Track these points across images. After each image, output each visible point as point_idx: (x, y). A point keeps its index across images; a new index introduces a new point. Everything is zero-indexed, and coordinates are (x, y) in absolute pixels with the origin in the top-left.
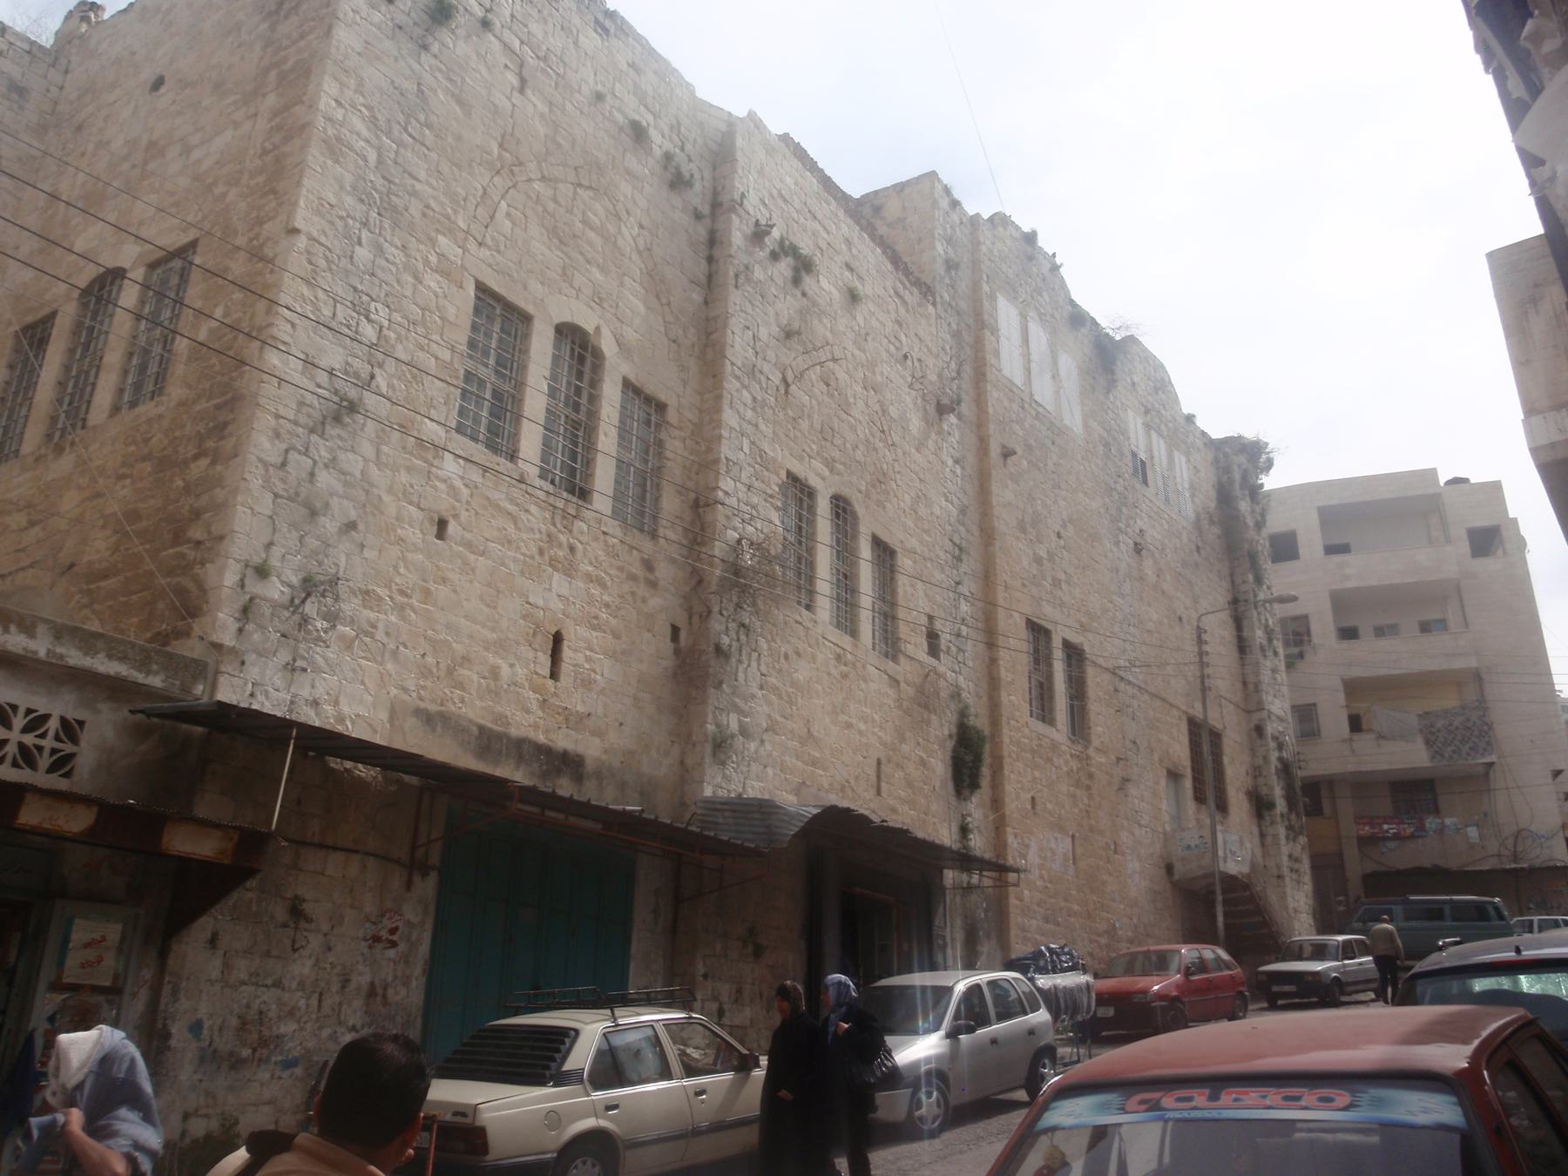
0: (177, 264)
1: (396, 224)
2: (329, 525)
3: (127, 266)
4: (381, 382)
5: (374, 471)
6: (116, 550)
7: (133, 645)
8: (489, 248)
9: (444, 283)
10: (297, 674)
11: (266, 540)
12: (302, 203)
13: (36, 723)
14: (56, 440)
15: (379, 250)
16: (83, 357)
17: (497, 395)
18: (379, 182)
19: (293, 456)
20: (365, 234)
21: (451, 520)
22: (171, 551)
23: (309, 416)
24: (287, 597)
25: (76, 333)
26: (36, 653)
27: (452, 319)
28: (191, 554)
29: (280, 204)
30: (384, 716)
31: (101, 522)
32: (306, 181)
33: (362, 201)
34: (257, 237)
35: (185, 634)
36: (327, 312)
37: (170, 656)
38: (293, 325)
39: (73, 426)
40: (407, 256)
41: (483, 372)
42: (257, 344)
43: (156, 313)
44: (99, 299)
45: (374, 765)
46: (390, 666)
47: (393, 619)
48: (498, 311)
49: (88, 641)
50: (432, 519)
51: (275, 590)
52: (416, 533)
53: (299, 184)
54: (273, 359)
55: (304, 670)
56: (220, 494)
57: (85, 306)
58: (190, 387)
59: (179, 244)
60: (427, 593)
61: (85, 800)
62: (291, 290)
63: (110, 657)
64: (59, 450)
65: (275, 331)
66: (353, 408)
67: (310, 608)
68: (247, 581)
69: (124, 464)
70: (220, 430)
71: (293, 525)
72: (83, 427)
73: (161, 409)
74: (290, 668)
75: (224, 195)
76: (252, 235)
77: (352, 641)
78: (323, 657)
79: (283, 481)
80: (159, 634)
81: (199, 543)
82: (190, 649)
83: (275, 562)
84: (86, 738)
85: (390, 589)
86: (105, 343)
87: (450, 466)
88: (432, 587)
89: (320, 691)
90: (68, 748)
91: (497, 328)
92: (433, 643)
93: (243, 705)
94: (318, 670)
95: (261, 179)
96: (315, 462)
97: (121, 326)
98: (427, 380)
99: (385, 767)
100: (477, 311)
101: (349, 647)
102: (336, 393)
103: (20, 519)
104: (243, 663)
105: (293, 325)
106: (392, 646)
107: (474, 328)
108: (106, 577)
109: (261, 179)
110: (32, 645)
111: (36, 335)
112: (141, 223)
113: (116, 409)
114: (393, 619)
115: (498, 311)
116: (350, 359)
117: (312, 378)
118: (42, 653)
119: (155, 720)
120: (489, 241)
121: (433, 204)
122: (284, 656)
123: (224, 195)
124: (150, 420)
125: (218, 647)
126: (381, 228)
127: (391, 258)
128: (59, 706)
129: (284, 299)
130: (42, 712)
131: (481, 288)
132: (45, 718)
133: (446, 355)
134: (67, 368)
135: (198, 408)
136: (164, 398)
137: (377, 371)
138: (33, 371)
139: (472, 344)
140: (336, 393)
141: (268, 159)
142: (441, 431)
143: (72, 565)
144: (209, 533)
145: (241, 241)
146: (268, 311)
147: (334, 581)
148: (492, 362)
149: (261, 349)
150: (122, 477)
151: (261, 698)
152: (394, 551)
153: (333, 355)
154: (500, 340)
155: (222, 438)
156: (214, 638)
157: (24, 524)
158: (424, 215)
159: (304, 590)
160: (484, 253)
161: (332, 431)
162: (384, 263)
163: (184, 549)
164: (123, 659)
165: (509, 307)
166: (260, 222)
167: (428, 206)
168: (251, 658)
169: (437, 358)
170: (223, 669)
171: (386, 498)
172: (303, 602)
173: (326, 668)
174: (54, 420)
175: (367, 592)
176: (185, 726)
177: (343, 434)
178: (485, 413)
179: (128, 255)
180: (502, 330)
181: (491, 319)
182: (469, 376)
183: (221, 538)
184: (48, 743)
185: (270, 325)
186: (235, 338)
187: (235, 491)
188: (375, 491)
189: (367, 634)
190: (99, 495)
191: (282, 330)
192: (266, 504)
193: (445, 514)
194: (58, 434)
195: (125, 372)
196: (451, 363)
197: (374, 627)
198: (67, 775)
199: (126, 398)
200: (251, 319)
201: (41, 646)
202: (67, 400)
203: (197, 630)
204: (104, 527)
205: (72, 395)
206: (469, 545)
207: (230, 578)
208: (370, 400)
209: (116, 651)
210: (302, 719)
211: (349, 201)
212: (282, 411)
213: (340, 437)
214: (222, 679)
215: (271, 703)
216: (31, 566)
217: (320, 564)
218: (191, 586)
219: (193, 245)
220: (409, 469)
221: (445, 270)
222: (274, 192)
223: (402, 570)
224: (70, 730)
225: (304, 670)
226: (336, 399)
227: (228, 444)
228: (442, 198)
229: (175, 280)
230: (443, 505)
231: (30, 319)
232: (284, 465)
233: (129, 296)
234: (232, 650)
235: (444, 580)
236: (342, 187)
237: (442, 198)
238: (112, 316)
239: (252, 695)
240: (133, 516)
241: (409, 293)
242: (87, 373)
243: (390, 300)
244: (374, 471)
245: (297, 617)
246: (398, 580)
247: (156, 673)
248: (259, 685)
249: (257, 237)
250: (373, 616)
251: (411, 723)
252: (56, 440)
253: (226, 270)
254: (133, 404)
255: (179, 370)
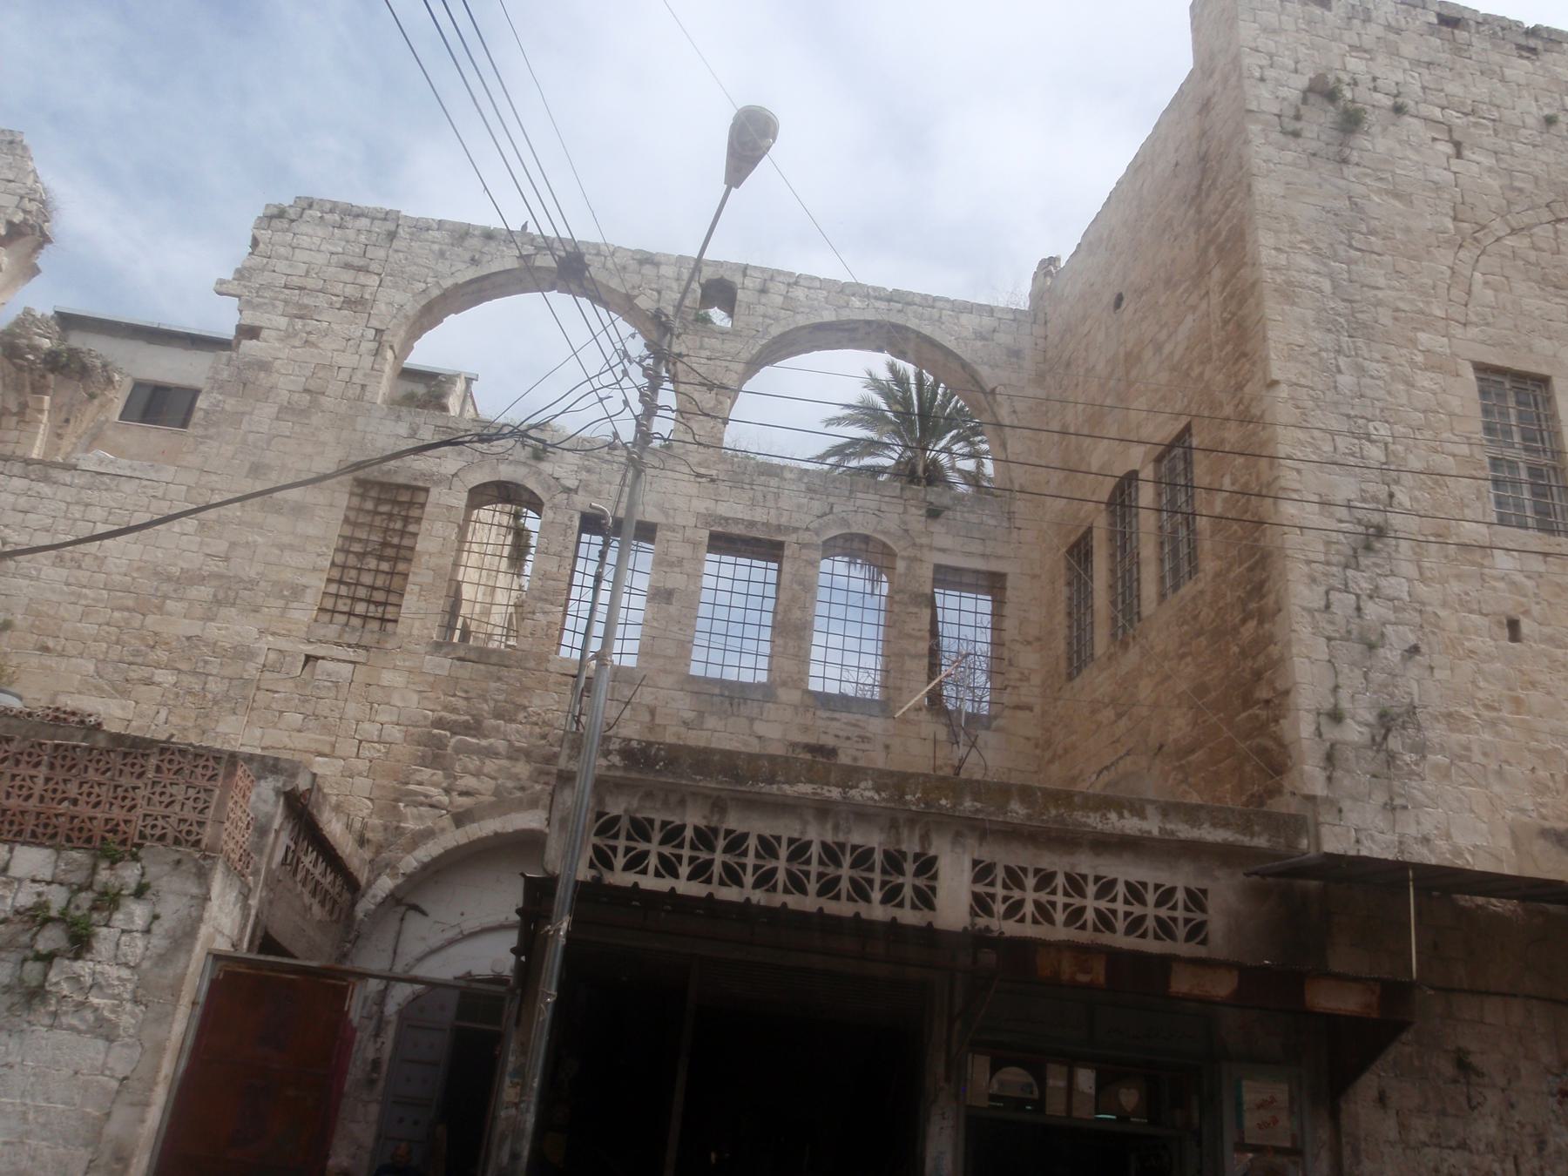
0: (1178, 451)
1: (1370, 339)
2: (1391, 655)
3: (1137, 467)
4: (1402, 497)
5: (1422, 590)
6: (1195, 724)
7: (1233, 811)
8: (1477, 325)
9: (1439, 377)
10: (1398, 813)
11: (1331, 685)
12: (1272, 355)
13: (1166, 896)
14: (1122, 637)
15: (1361, 370)
16: (1123, 558)
17: (1535, 472)
18: (1342, 307)
19: (1334, 596)
20: (1342, 361)
21: (1521, 617)
22: (1244, 715)
23: (1338, 553)
24: (1368, 737)
25: (1111, 539)
26: (1150, 832)
27: (1458, 410)
28: (1263, 714)
29: (1254, 364)
30: (1505, 842)
31: (1176, 702)
32: (1270, 334)
33: (1329, 330)
34: (1241, 401)
35: (1275, 792)
36: (1328, 448)
37: (1269, 815)
38: (1299, 471)
39: (1131, 621)
40: (1391, 365)
41: (1509, 454)
42: (1270, 500)
43: (1173, 501)
44: (1122, 504)
45: (1509, 898)
46: (1497, 788)
47: (1487, 736)
48: (1507, 385)
49: (1191, 814)
50: (1500, 623)
51: (1353, 732)
52: (1488, 641)
53: (1265, 339)
54: (1289, 509)
55: (1405, 808)
56: (1274, 651)
57: (1113, 513)
58: (1219, 558)
59: (1175, 433)
60: (1517, 702)
61: (1227, 965)
62: (1287, 442)
63: (1214, 825)
64: (1125, 645)
65: (1283, 483)
66: (1381, 532)
67: (1394, 743)
68: (1323, 729)
69: (1182, 644)
70: (1258, 590)
71: (1353, 664)
72: (1139, 620)
73: (1201, 586)
74: (1390, 808)
75: (1201, 374)
76: (1236, 401)
77: (1448, 769)
78: (1423, 792)
79: (1332, 623)
80: (1252, 796)
81: (1267, 702)
82: (1284, 805)
83: (1345, 704)
84: (1212, 904)
85: (1474, 706)
86: (1138, 539)
87: (1503, 562)
88: (1521, 693)
89: (1428, 827)
90: (1198, 916)
91: (1511, 401)
92: (1543, 755)
93: (1352, 853)
94: (1419, 806)
95: (1229, 348)
96: (1358, 596)
97: (1147, 522)
98: (1450, 482)
99: (1523, 899)
100: (1483, 393)
101: (1446, 775)
102: (1359, 522)
103: (1109, 713)
104: (1340, 811)
105: (1299, 471)
106: (1494, 766)
107: (1486, 411)
108: (1193, 751)
109: (1229, 348)
110: (1145, 825)
111: (1080, 552)
112: (1139, 426)
113: (1162, 596)
114: (1487, 736)
115: (1507, 385)
116: (1364, 486)
117: (1331, 515)
118: (1155, 832)
119: (1270, 880)
120: (1473, 318)
121: (1402, 305)
122: (1380, 798)
123: (1201, 374)
124: (1194, 598)
125: (1311, 799)
126: (1356, 349)
127: (1375, 373)
128: (1181, 878)
129: (1283, 450)
130: (1168, 885)
131: (1481, 369)
132: (1172, 890)
133: (1464, 450)
134: (1113, 571)
135: (1232, 575)
136: (1201, 575)
137: (1395, 488)
138: (1086, 583)
139: (1489, 429)
140: (1359, 522)
141: (1230, 327)
142: (1483, 529)
143: (1161, 747)
144: (1274, 689)
145: (1228, 410)
146: (1271, 467)
147: (1412, 710)
148: (1517, 439)
149: (1275, 504)
150: (1182, 657)
151: (1368, 843)
152: (1468, 666)
153: (1346, 488)
154: (1520, 415)
155: (1262, 597)
156: (1306, 791)
157: (1113, 717)
158: (1396, 319)
159: (1383, 726)
160: (1473, 332)
161: (1365, 561)
162: (1368, 381)
163: (1256, 710)
164: (1226, 825)
165: (1520, 377)
166: (1240, 387)
167: (1397, 310)
168: (1346, 805)
169: (1454, 456)
170: (1321, 819)
171: (1442, 613)
172: (1385, 738)
173: (1426, 801)
174: (1114, 620)
175: (1450, 715)
176: (1301, 882)
177: (1379, 561)
178: (1526, 495)
179: (1137, 458)
180: (1519, 403)
181: (1502, 396)
182: (1495, 463)
183: (1287, 693)
184: (1180, 914)
185: (1277, 478)
186: (1248, 501)
187: (1288, 644)
188: (1429, 609)
189: (1461, 758)
190: (1168, 677)
191: (1289, 478)
192: (1321, 650)
193: (1513, 614)
194: (1120, 632)
195: (1162, 561)
196: (1472, 456)
197: (1468, 749)
198: (1203, 942)
199: (1168, 583)
200: (1258, 478)
201: (1152, 825)
202: (1120, 599)
203: (1287, 787)
204: (1179, 705)
205: (1123, 593)
206: (1551, 640)
207: (1306, 729)
208: (1396, 520)
209: (1219, 818)
210: (1416, 859)
211: (1317, 335)
212: (1312, 556)
213: (1376, 565)
214: (1325, 830)
215: (1380, 846)
216: (1128, 754)
217: (1392, 696)
218: (1271, 744)
219: (1187, 429)
220: (1458, 577)
221: (1435, 365)
222: (1244, 355)
223: (1482, 684)
224: (1196, 899)
225: (1405, 808)
226: (1361, 529)
227: (1270, 600)
228: (1409, 296)
229: (1181, 466)
230: (1509, 606)
231: (1073, 539)
232: (1328, 607)
233: (1146, 495)
234: (1327, 800)
235: (1533, 684)
236: (1305, 326)
237: (1409, 296)
238: (1137, 515)
239: (1358, 841)
240: (1201, 690)
241: (1404, 401)
242: (1130, 571)
243: (1387, 414)
244: (1422, 590)
245: (1382, 755)
246: (1480, 695)
247: (1260, 834)
248: (1360, 829)
249: (1241, 401)
250: (1463, 738)
251: (1539, 845)
252: (1122, 637)
253: (1222, 441)
254: (1176, 587)
255: (1206, 545)
